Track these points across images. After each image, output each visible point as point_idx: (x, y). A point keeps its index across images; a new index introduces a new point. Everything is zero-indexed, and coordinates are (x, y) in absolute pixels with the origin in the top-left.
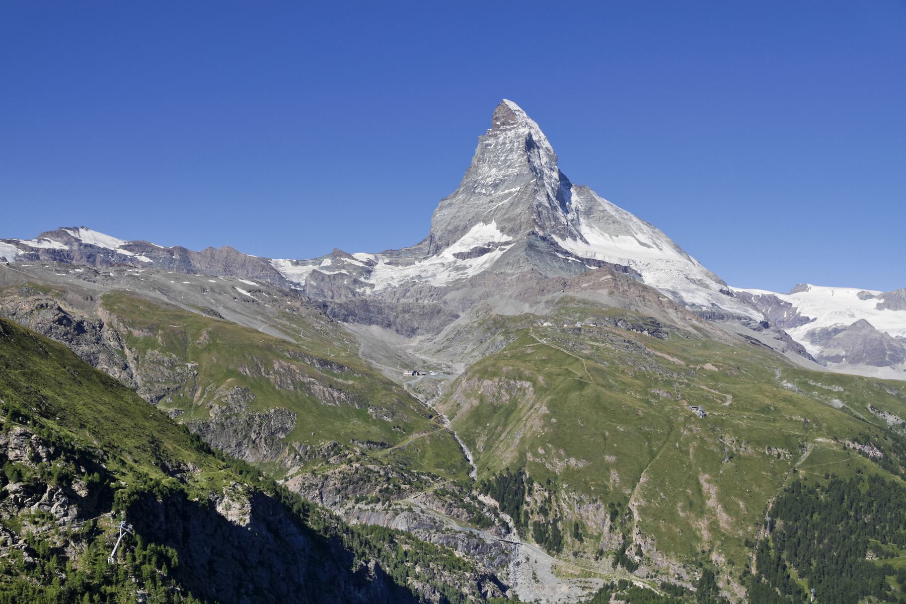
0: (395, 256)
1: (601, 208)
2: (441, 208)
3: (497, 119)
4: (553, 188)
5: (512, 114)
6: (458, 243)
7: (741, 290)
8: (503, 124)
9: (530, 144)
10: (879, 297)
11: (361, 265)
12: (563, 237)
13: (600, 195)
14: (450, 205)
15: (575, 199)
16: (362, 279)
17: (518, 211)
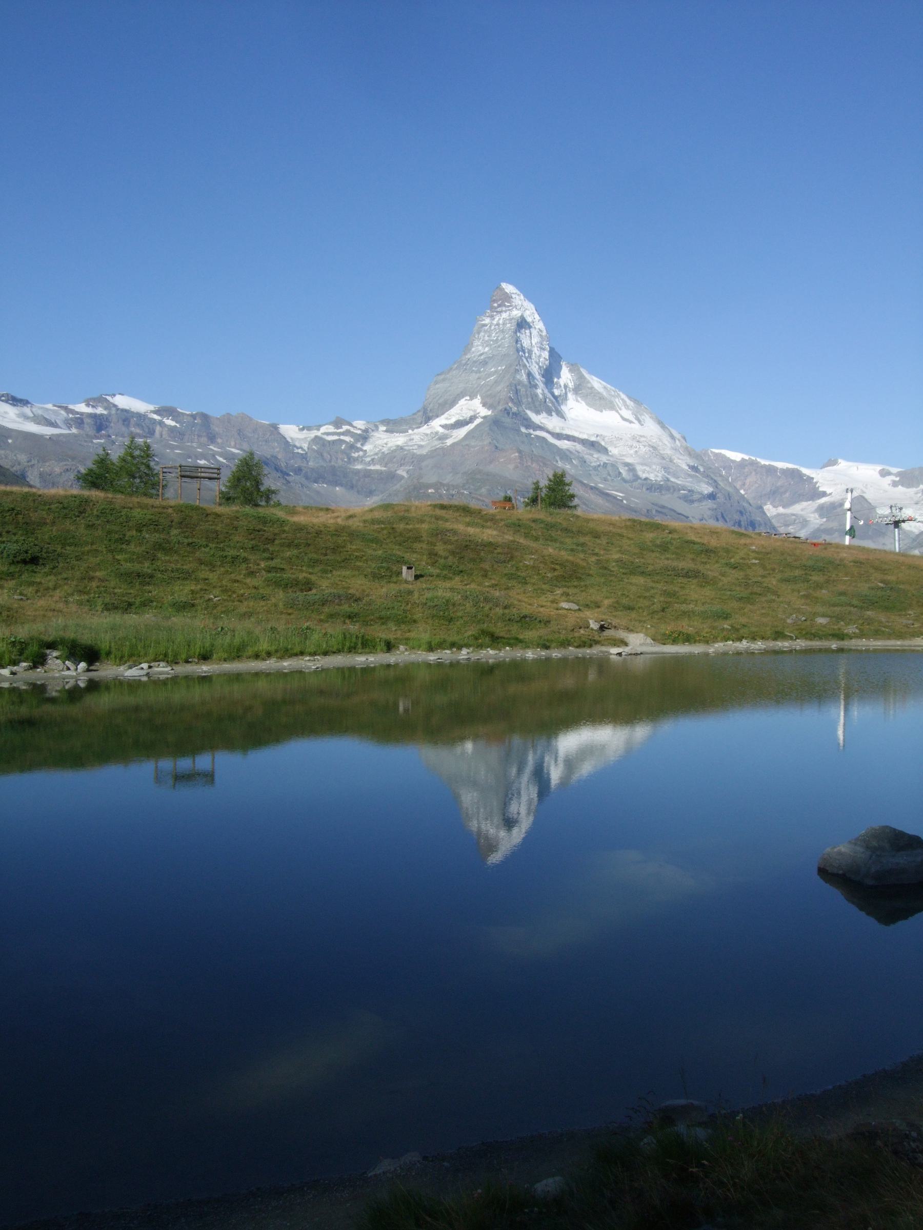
0: (394, 426)
1: (589, 385)
2: (436, 383)
3: (494, 301)
4: (540, 367)
5: (508, 298)
6: (446, 415)
7: (767, 463)
8: (499, 306)
9: (522, 324)
10: (897, 475)
11: (359, 432)
12: (538, 412)
13: (590, 373)
14: (444, 380)
15: (566, 376)
16: (359, 445)
17: (499, 388)
